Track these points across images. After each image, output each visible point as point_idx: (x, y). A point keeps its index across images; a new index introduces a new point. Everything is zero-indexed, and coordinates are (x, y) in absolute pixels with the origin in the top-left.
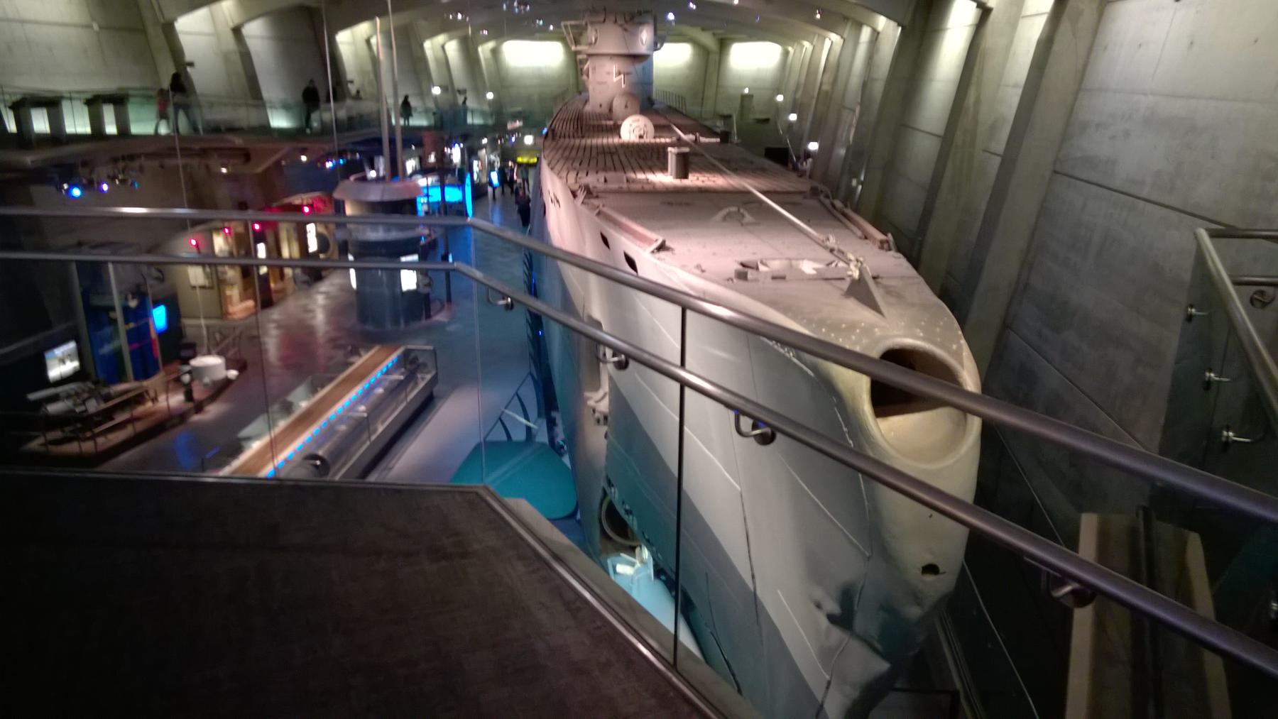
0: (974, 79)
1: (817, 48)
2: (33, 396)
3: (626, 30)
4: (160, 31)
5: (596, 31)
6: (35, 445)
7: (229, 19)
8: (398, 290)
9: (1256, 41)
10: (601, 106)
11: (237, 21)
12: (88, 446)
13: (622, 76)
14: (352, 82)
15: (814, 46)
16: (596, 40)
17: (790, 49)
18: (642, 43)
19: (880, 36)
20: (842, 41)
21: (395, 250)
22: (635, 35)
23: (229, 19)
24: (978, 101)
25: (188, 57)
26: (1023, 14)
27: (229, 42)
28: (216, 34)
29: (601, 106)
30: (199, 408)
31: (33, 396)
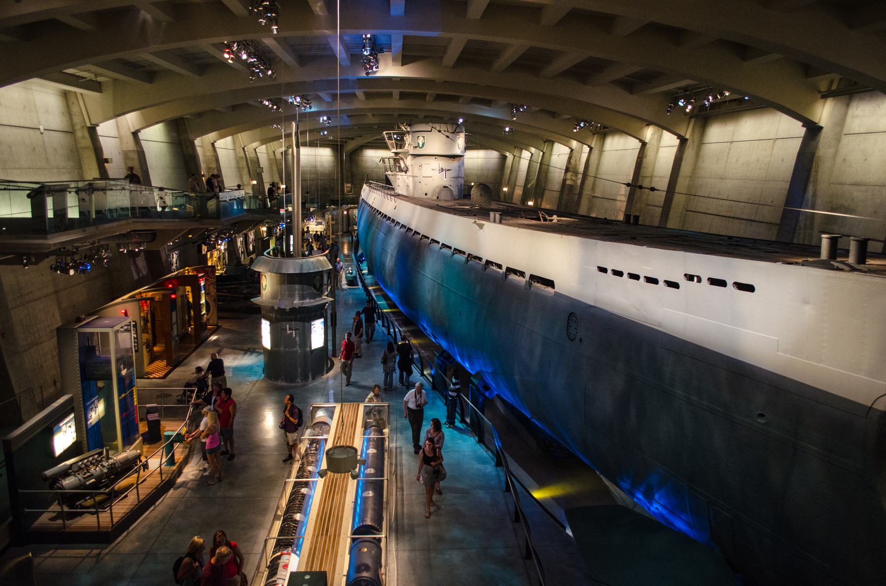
0: (812, 179)
1: (547, 155)
2: (49, 472)
3: (447, 137)
4: (87, 135)
5: (424, 137)
6: (44, 519)
7: (130, 124)
8: (308, 349)
9: (782, 160)
10: (426, 194)
11: (137, 128)
12: (105, 518)
13: (444, 172)
14: (203, 176)
15: (544, 153)
16: (423, 144)
17: (508, 154)
18: (459, 147)
19: (647, 146)
20: (589, 149)
21: (306, 316)
22: (454, 141)
23: (130, 124)
24: (815, 195)
25: (106, 155)
26: (846, 131)
27: (130, 144)
28: (119, 137)
29: (426, 194)
30: (179, 472)
31: (49, 472)
